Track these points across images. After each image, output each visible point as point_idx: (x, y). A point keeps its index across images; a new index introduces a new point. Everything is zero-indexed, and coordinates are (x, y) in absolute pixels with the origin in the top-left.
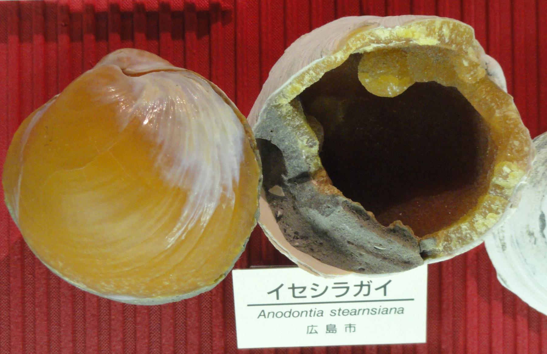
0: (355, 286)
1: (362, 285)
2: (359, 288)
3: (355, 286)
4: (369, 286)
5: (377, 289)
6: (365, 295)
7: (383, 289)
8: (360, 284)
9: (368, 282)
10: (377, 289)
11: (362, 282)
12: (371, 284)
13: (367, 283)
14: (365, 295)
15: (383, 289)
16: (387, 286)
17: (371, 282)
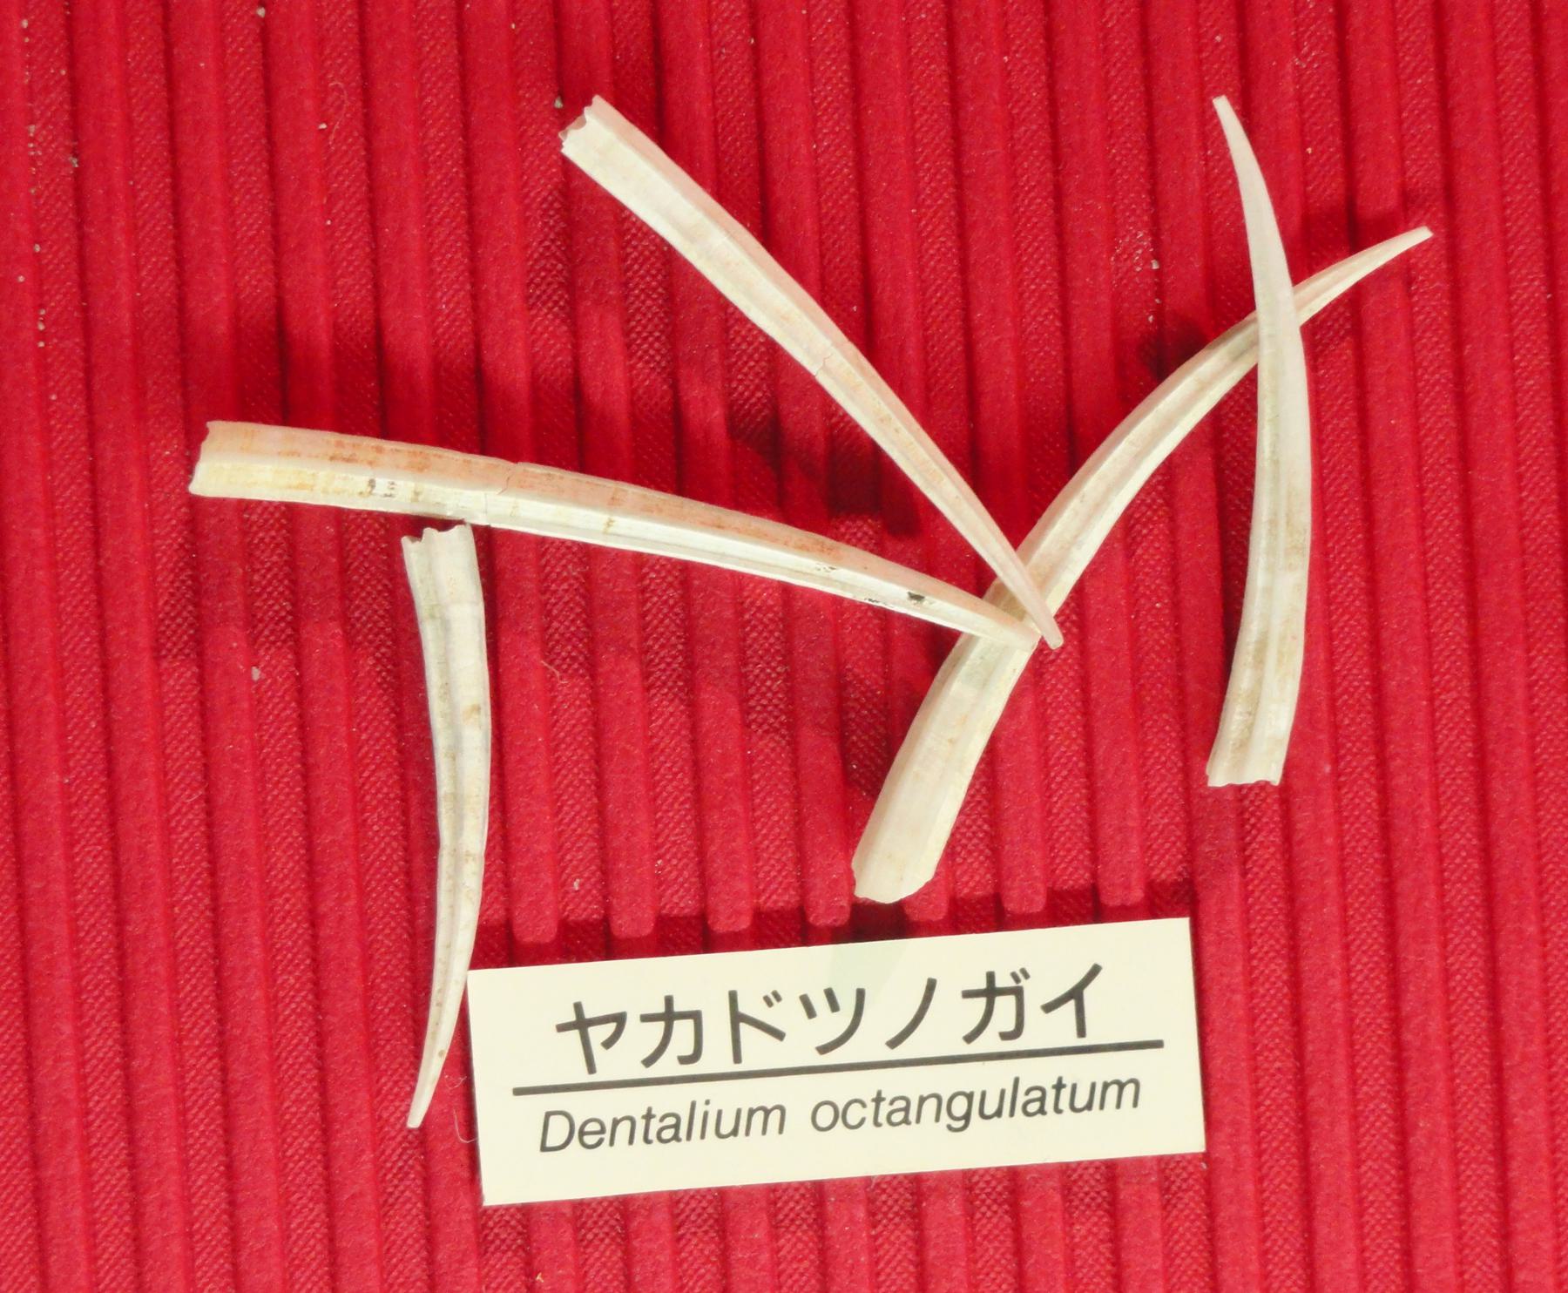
0: (968, 994)
1: (991, 992)
2: (981, 1003)
3: (968, 994)
4: (1018, 992)
5: (1049, 1008)
6: (1005, 1036)
7: (1070, 1006)
8: (983, 985)
9: (1017, 980)
10: (1049, 1008)
11: (991, 977)
12: (1024, 983)
13: (1011, 983)
14: (1005, 1036)
15: (1071, 1005)
16: (1088, 993)
17: (1027, 976)
